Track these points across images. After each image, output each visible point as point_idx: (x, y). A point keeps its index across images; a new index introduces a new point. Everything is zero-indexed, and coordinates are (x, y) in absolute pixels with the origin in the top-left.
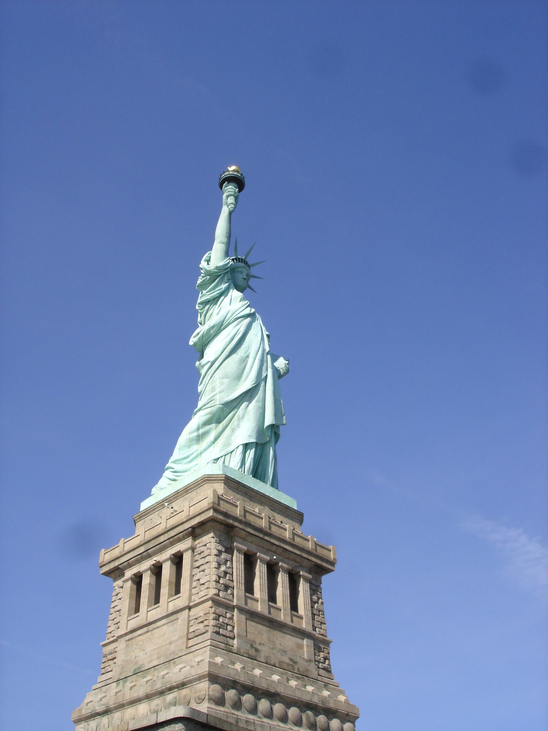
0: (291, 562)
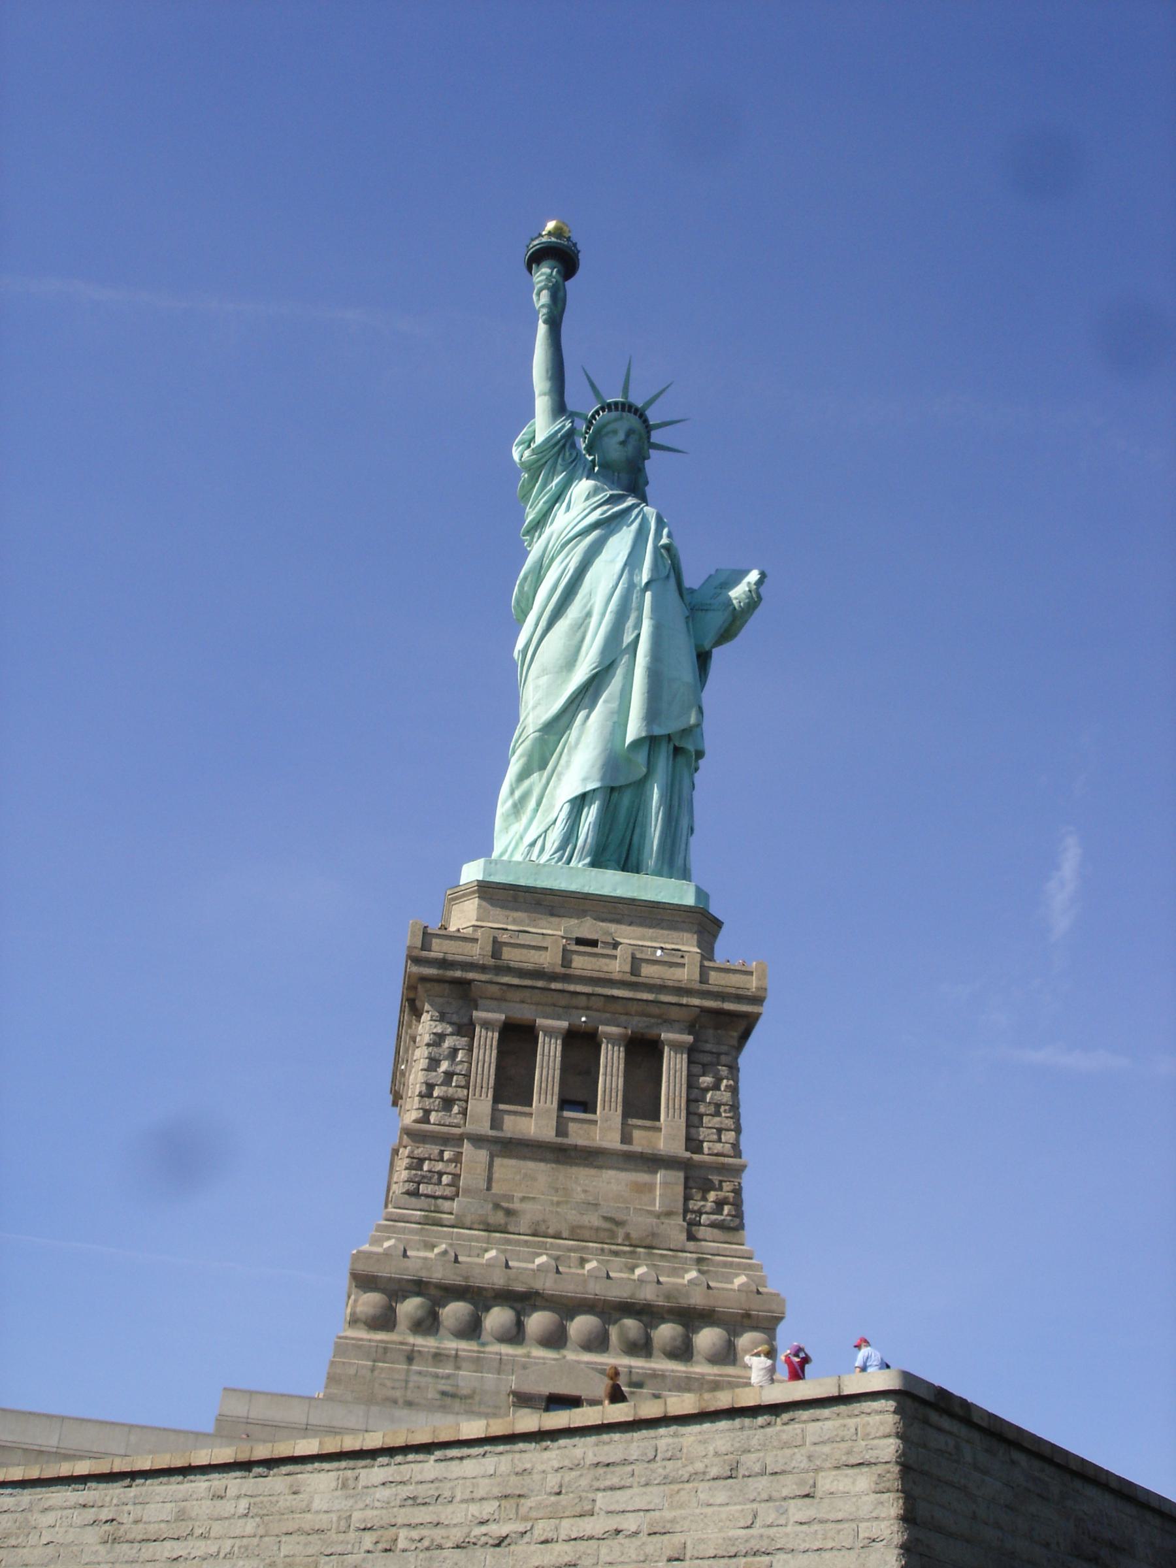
0: (637, 1018)
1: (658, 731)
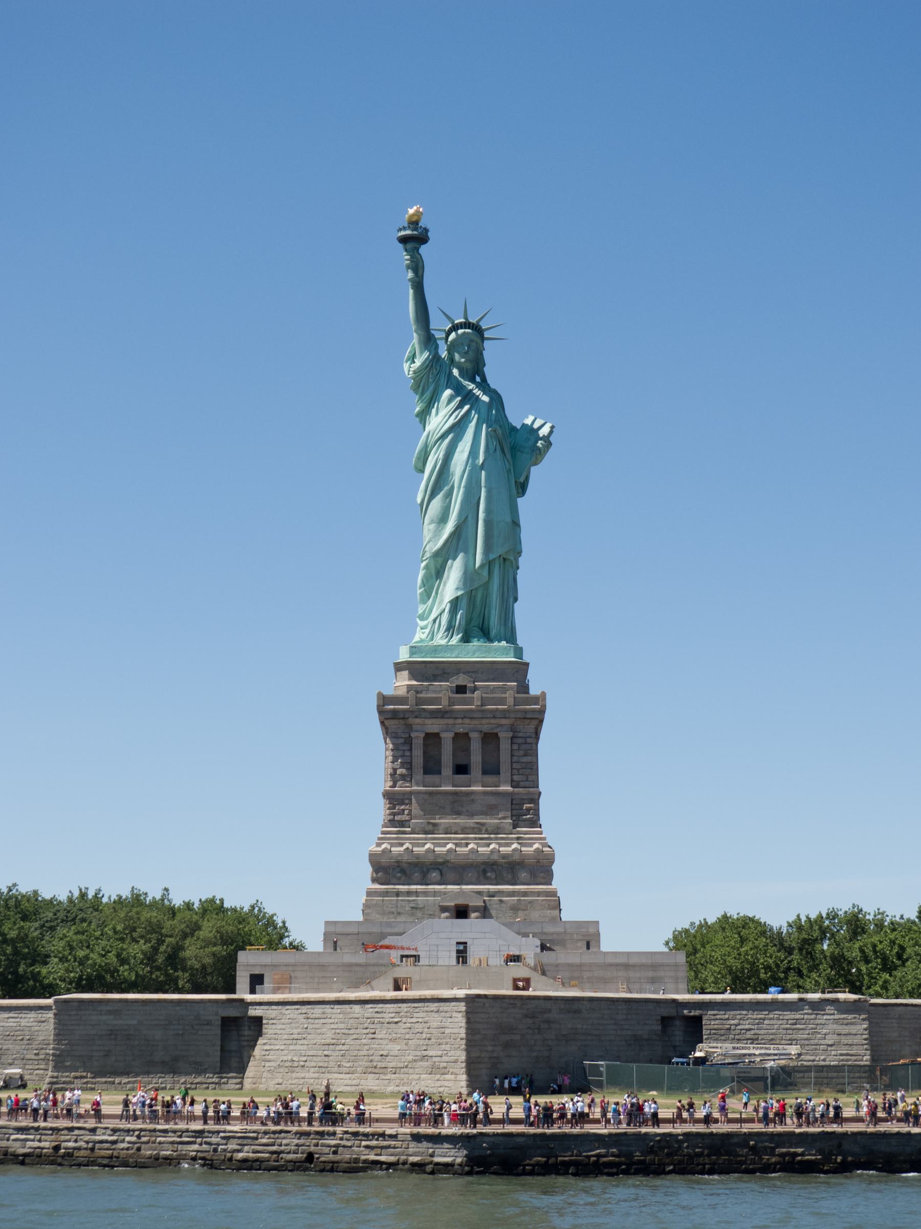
1: (492, 557)
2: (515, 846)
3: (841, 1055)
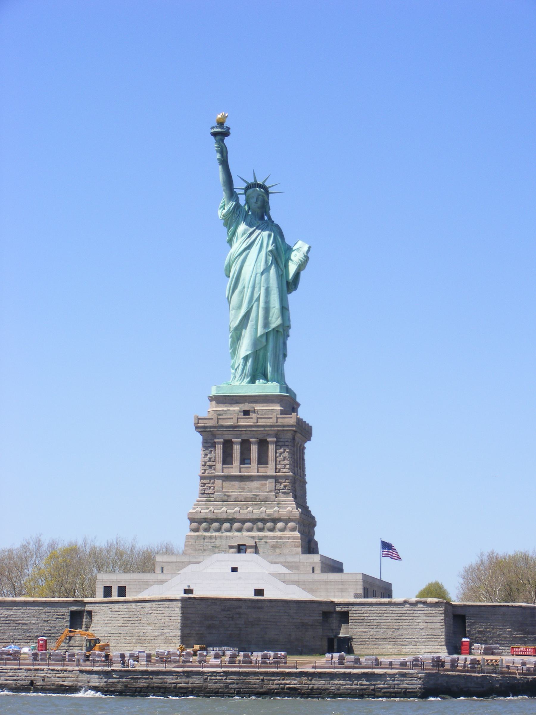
2: (276, 508)
3: (427, 635)
